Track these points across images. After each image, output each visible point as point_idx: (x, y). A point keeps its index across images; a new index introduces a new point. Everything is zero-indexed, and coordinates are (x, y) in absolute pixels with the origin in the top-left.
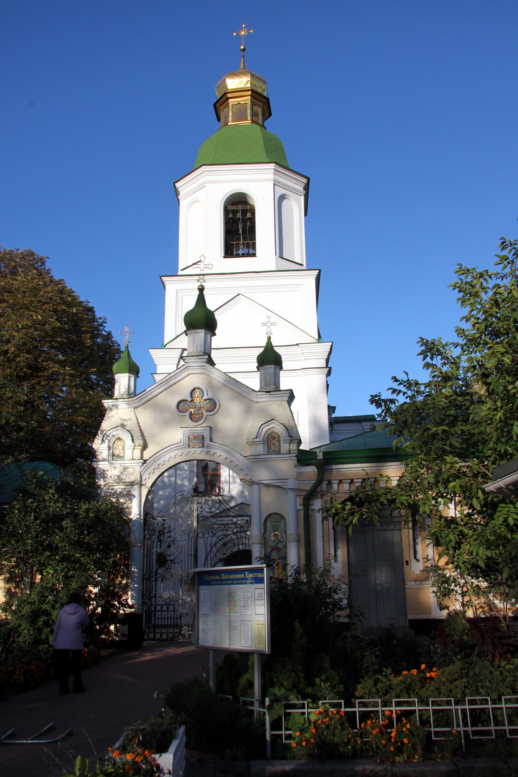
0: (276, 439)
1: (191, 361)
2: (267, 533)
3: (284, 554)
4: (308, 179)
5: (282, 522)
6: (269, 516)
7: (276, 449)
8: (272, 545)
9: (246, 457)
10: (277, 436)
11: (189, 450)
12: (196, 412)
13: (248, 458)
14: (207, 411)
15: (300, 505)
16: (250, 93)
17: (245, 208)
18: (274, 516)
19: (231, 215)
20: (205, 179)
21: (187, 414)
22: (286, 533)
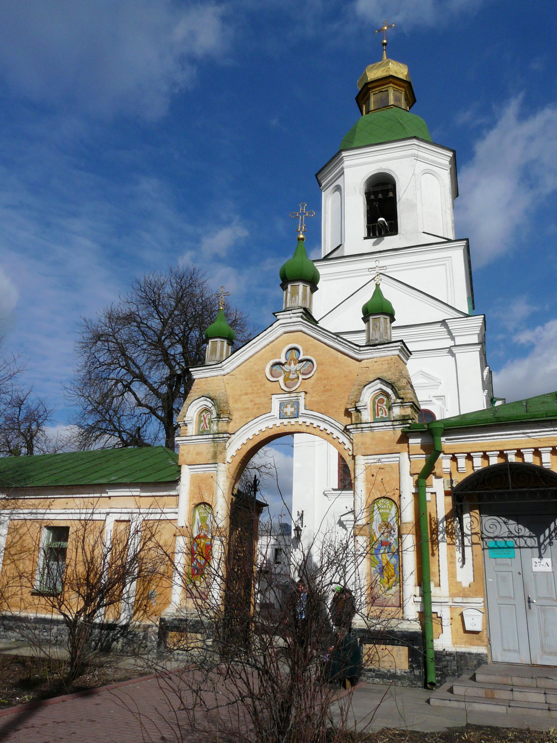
0: (385, 403)
7: (384, 415)
14: (303, 374)
19: (372, 197)
21: (281, 379)
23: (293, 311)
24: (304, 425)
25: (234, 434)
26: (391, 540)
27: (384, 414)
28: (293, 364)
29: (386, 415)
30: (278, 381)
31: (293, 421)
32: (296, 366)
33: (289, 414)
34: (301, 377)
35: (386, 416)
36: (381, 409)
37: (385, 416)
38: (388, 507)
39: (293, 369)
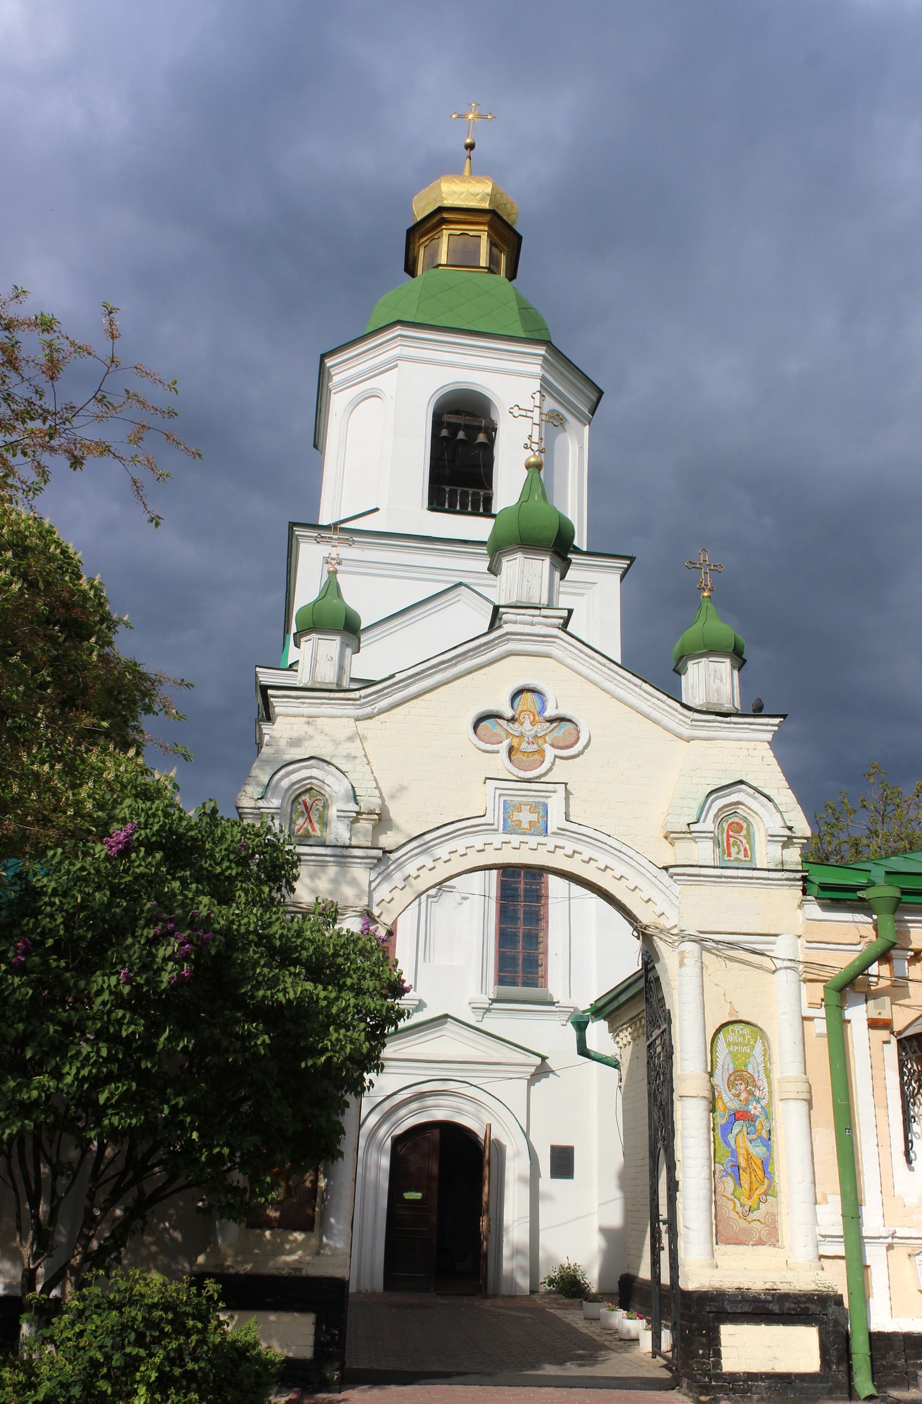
0: (744, 832)
1: (519, 618)
2: (718, 1072)
3: (764, 1134)
5: (759, 1047)
8: (734, 1105)
9: (666, 868)
10: (745, 825)
11: (507, 837)
12: (524, 746)
13: (671, 870)
14: (552, 745)
15: (811, 1005)
16: (487, 218)
18: (737, 1027)
21: (503, 747)
22: (768, 1072)
25: (390, 852)
26: (755, 1108)
27: (742, 853)
28: (527, 723)
29: (746, 856)
30: (498, 752)
31: (533, 841)
32: (536, 727)
33: (526, 826)
34: (550, 752)
35: (747, 859)
36: (735, 844)
37: (744, 859)
38: (749, 1041)
39: (529, 733)
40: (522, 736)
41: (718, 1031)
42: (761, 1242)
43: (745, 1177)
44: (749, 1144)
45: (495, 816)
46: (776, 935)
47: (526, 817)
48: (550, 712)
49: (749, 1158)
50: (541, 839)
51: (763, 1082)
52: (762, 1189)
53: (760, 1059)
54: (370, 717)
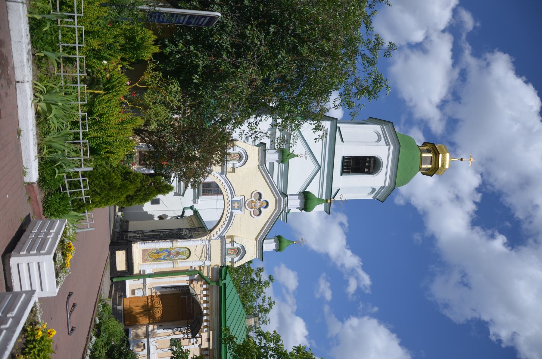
0: (234, 253)
2: (179, 249)
3: (166, 258)
4: (382, 202)
6: (189, 250)
8: (172, 251)
11: (230, 201)
12: (254, 204)
15: (195, 268)
17: (371, 168)
19: (368, 159)
20: (392, 147)
21: (253, 199)
22: (180, 259)
23: (286, 207)
24: (228, 205)
28: (260, 204)
31: (230, 207)
34: (252, 210)
40: (256, 203)
41: (188, 249)
42: (143, 258)
43: (156, 255)
44: (163, 255)
45: (235, 198)
46: (210, 260)
47: (236, 205)
48: (262, 209)
49: (160, 255)
50: (230, 209)
51: (177, 258)
52: (154, 258)
53: (182, 257)
54: (259, 168)
